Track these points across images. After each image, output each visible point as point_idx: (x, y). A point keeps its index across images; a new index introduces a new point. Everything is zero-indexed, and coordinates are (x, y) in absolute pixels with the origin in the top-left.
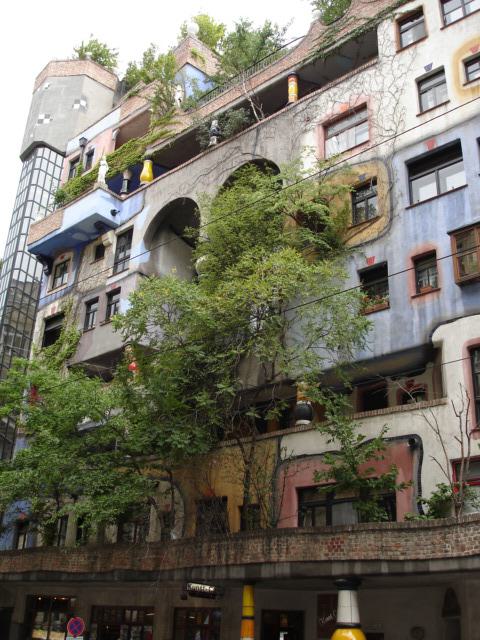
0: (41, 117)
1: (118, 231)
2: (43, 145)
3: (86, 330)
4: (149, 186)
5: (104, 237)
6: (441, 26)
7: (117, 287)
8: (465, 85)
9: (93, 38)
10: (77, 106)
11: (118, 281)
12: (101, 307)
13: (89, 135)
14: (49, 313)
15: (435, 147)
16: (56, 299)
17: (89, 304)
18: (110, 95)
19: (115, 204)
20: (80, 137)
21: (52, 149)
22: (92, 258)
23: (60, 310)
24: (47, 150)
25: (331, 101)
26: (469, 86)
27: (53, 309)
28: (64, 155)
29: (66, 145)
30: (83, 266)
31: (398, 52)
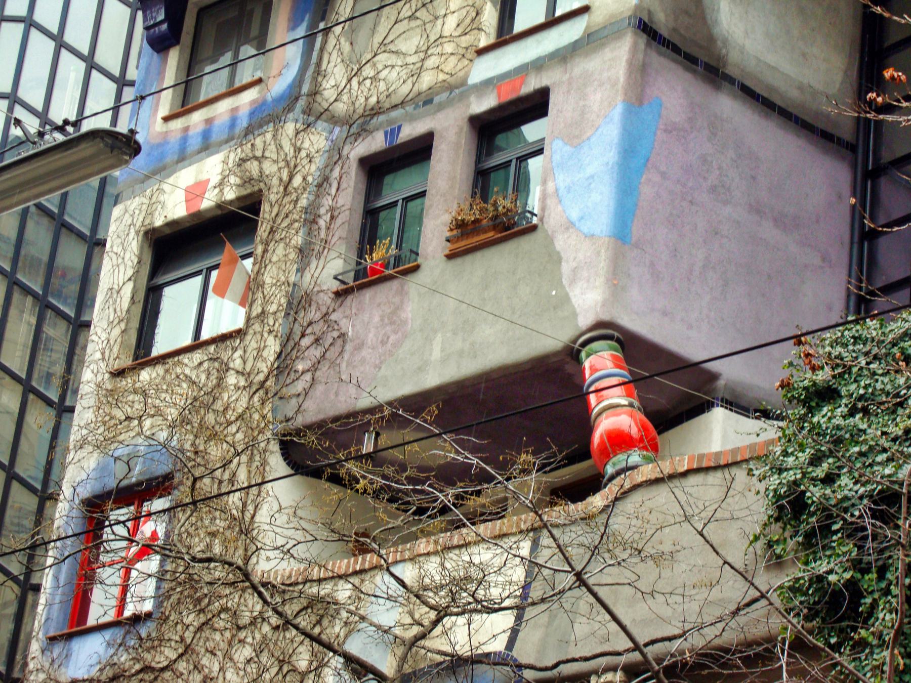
3: (363, 279)
7: (531, 85)
11: (538, 65)
12: (446, 181)
14: (173, 204)
16: (207, 147)
17: (377, 169)
23: (230, 195)
27: (195, 192)
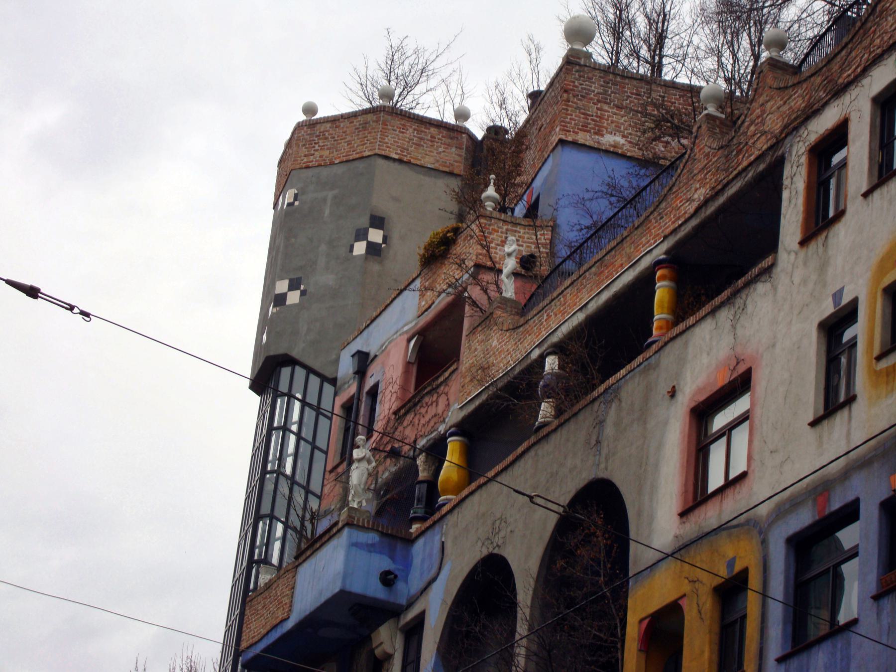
2: (289, 361)
13: (369, 342)
19: (392, 558)
28: (333, 381)
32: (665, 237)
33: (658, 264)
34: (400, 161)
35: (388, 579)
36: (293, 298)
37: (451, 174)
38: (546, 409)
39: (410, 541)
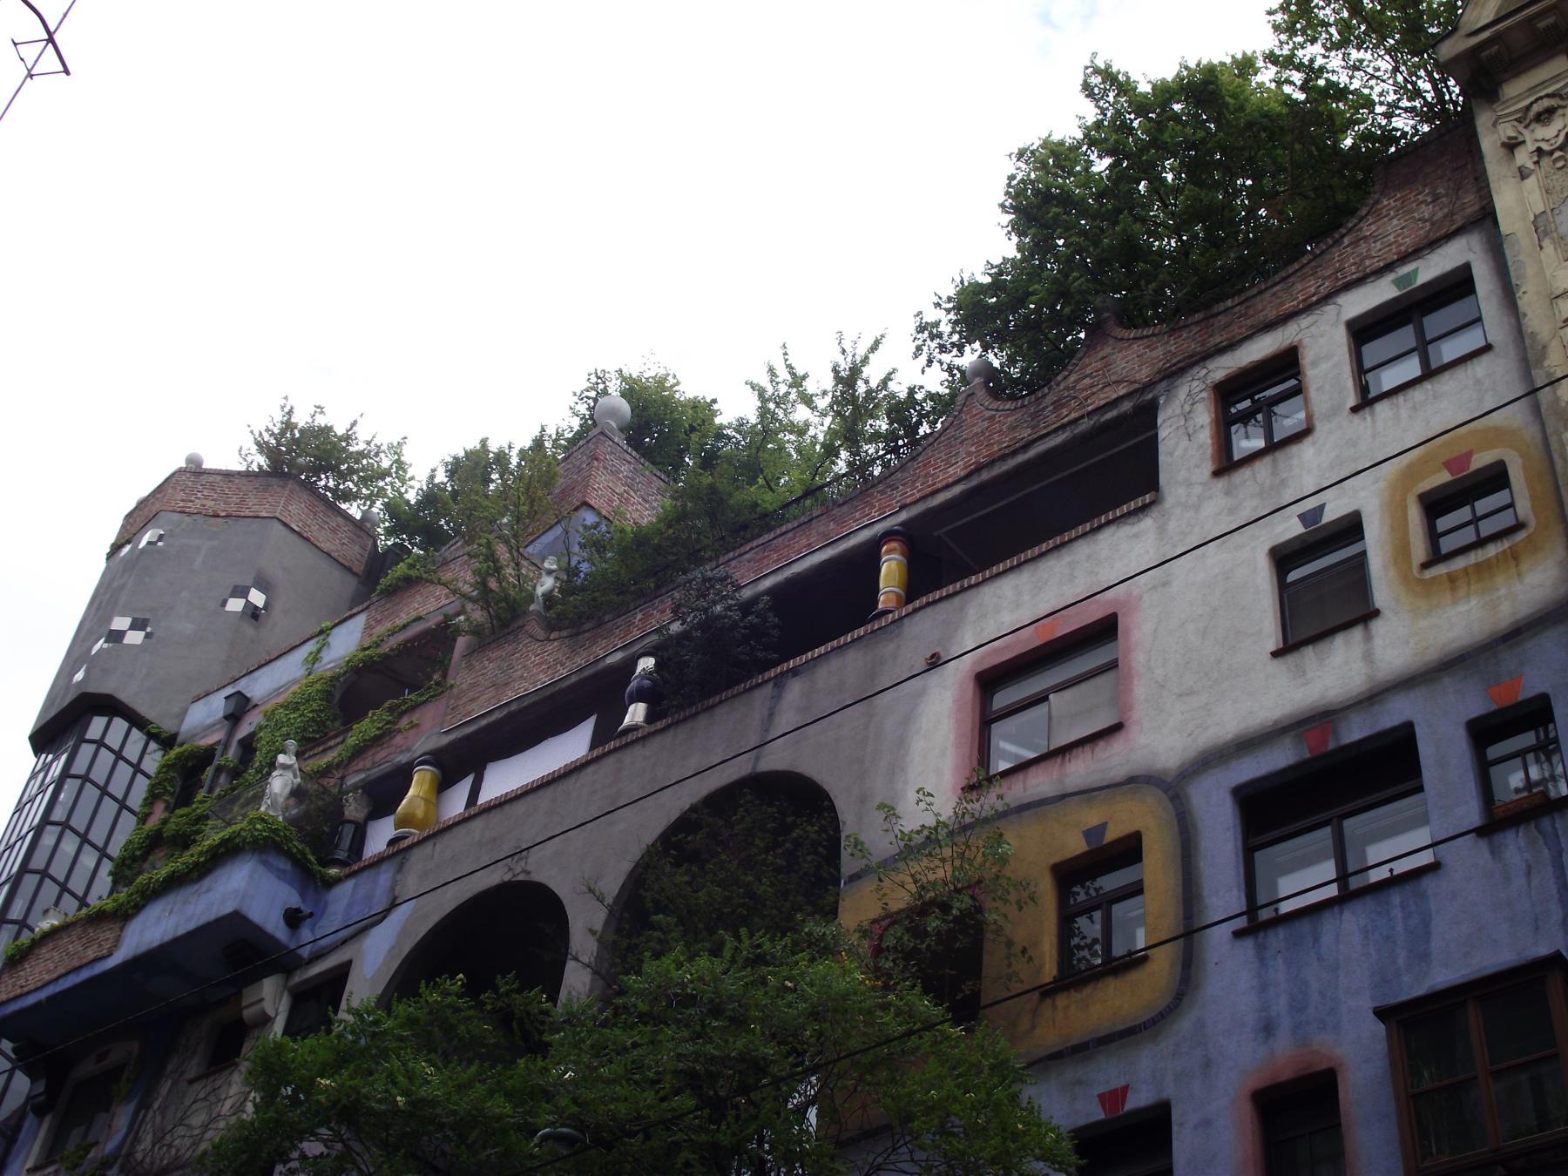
0: (121, 623)
1: (297, 978)
2: (110, 706)
4: (420, 843)
5: (249, 996)
6: (1352, 401)
8: (1425, 566)
9: (321, 421)
10: (235, 605)
15: (1332, 745)
18: (352, 583)
19: (302, 895)
20: (229, 691)
21: (136, 720)
22: (194, 1067)
24: (120, 725)
25: (1012, 605)
26: (1440, 570)
29: (185, 711)
30: (165, 1089)
31: (1217, 474)
32: (902, 508)
33: (888, 535)
34: (299, 534)
35: (293, 918)
36: (135, 638)
37: (349, 569)
38: (636, 713)
39: (330, 883)
